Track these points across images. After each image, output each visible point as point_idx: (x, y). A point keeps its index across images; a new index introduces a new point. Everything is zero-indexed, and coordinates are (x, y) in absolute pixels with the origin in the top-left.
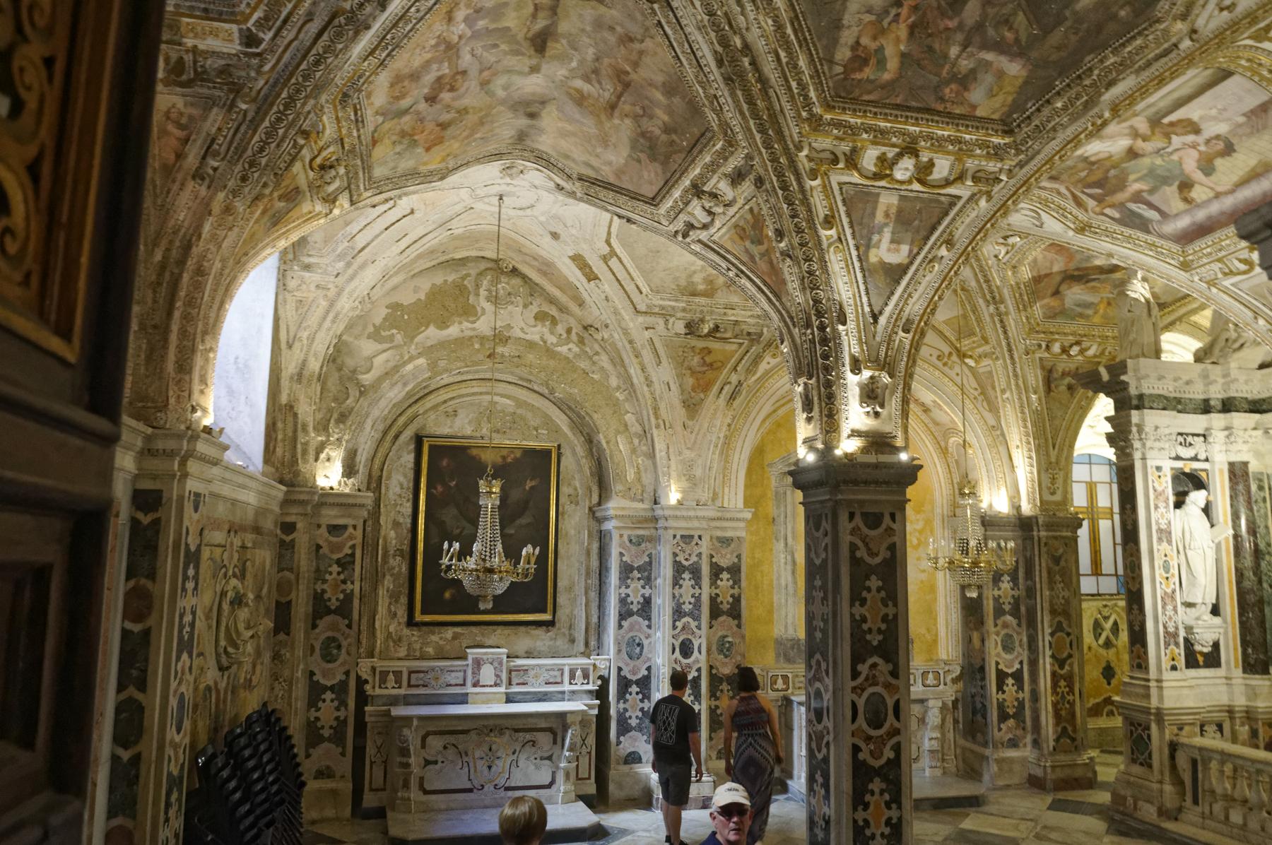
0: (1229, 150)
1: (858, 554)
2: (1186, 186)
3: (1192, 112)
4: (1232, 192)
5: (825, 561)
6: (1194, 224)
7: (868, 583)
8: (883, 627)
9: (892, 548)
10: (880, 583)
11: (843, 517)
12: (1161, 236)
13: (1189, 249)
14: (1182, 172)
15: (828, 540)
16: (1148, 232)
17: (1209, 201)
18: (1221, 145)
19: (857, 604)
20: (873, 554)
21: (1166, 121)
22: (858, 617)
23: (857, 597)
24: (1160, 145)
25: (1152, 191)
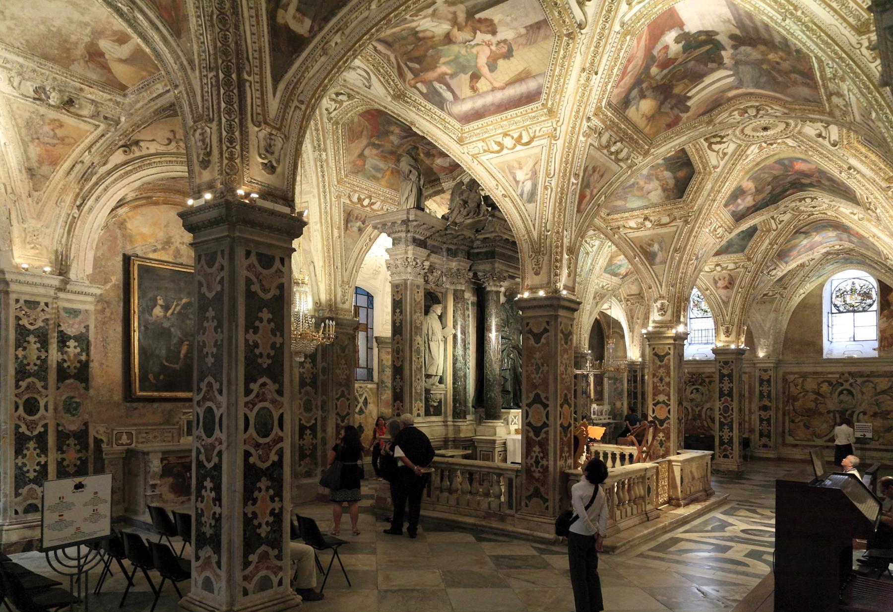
0: (509, 55)
1: (253, 288)
2: (476, 76)
4: (503, 88)
5: (220, 295)
6: (473, 109)
7: (260, 315)
8: (272, 353)
9: (281, 287)
10: (270, 316)
11: (240, 253)
12: (450, 114)
13: (467, 128)
14: (476, 66)
15: (225, 274)
16: (443, 110)
17: (486, 93)
18: (505, 49)
19: (251, 331)
20: (266, 291)
21: (477, 16)
22: (251, 343)
23: (251, 326)
24: (469, 37)
25: (453, 76)
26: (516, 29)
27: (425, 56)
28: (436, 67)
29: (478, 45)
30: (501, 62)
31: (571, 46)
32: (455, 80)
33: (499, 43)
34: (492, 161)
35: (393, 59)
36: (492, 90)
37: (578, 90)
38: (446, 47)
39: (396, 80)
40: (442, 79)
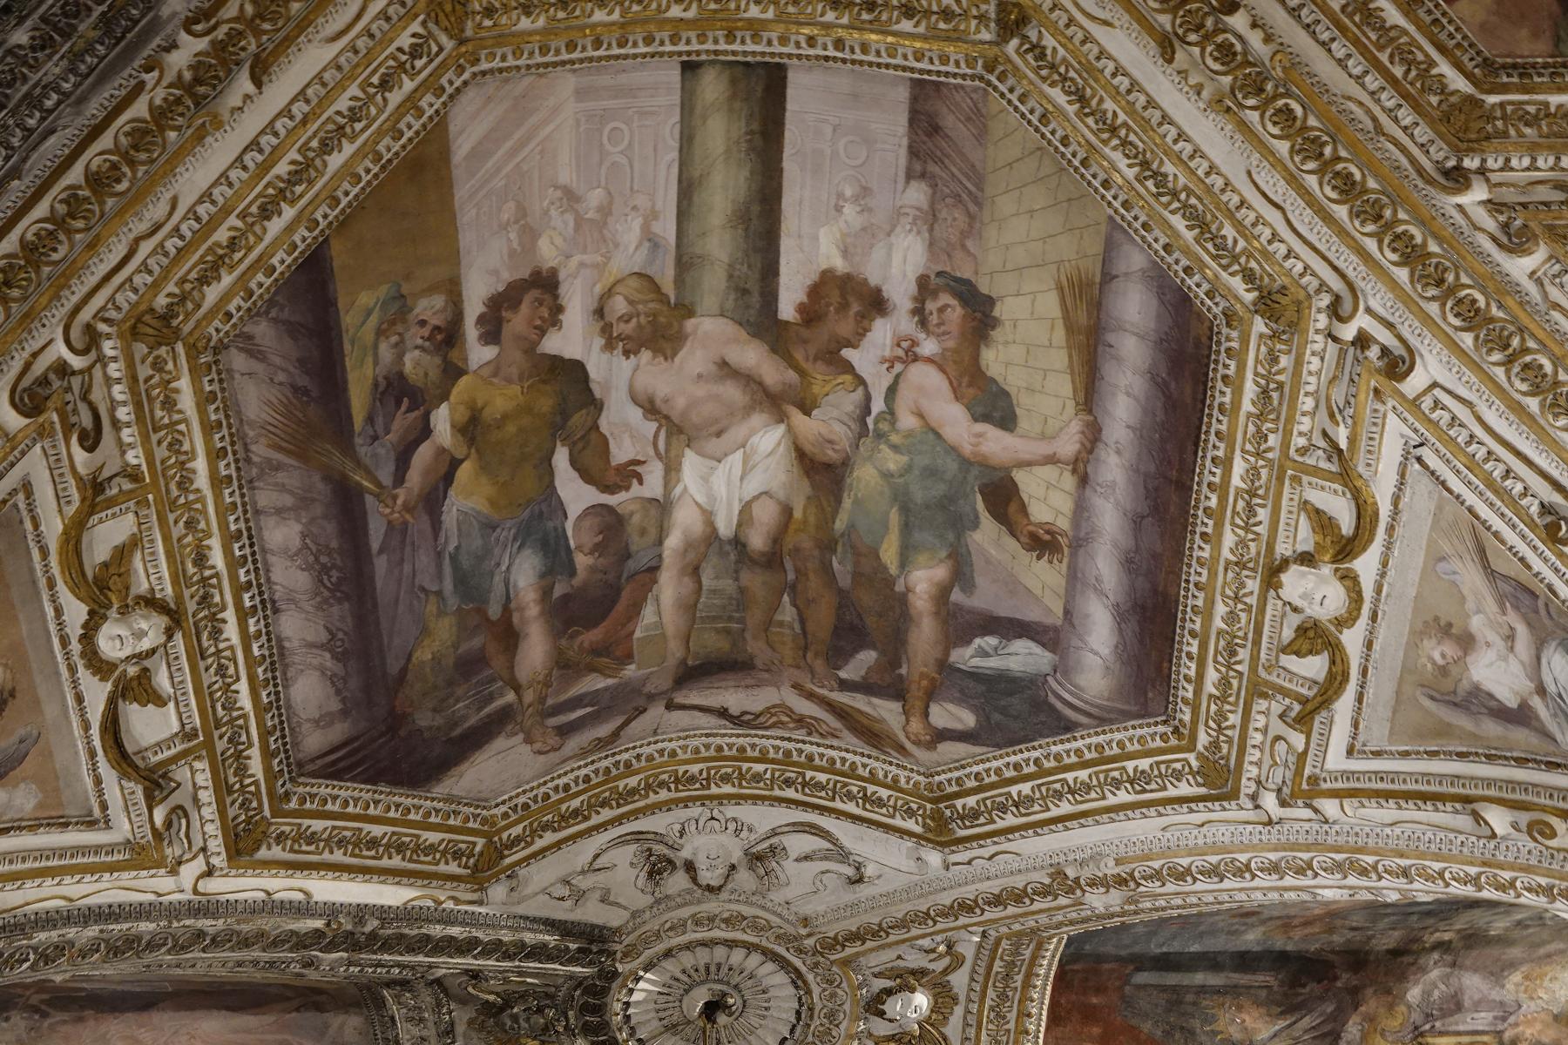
0: (980, 315)
2: (1002, 497)
3: (809, 250)
4: (1093, 435)
6: (1120, 616)
14: (966, 463)
17: (1081, 509)
21: (787, 309)
24: (849, 401)
25: (961, 573)
26: (899, 213)
27: (844, 600)
28: (903, 600)
29: (892, 391)
30: (993, 360)
31: (1049, 42)
32: (980, 580)
33: (919, 312)
36: (1084, 480)
37: (1243, 126)
38: (847, 503)
40: (963, 625)
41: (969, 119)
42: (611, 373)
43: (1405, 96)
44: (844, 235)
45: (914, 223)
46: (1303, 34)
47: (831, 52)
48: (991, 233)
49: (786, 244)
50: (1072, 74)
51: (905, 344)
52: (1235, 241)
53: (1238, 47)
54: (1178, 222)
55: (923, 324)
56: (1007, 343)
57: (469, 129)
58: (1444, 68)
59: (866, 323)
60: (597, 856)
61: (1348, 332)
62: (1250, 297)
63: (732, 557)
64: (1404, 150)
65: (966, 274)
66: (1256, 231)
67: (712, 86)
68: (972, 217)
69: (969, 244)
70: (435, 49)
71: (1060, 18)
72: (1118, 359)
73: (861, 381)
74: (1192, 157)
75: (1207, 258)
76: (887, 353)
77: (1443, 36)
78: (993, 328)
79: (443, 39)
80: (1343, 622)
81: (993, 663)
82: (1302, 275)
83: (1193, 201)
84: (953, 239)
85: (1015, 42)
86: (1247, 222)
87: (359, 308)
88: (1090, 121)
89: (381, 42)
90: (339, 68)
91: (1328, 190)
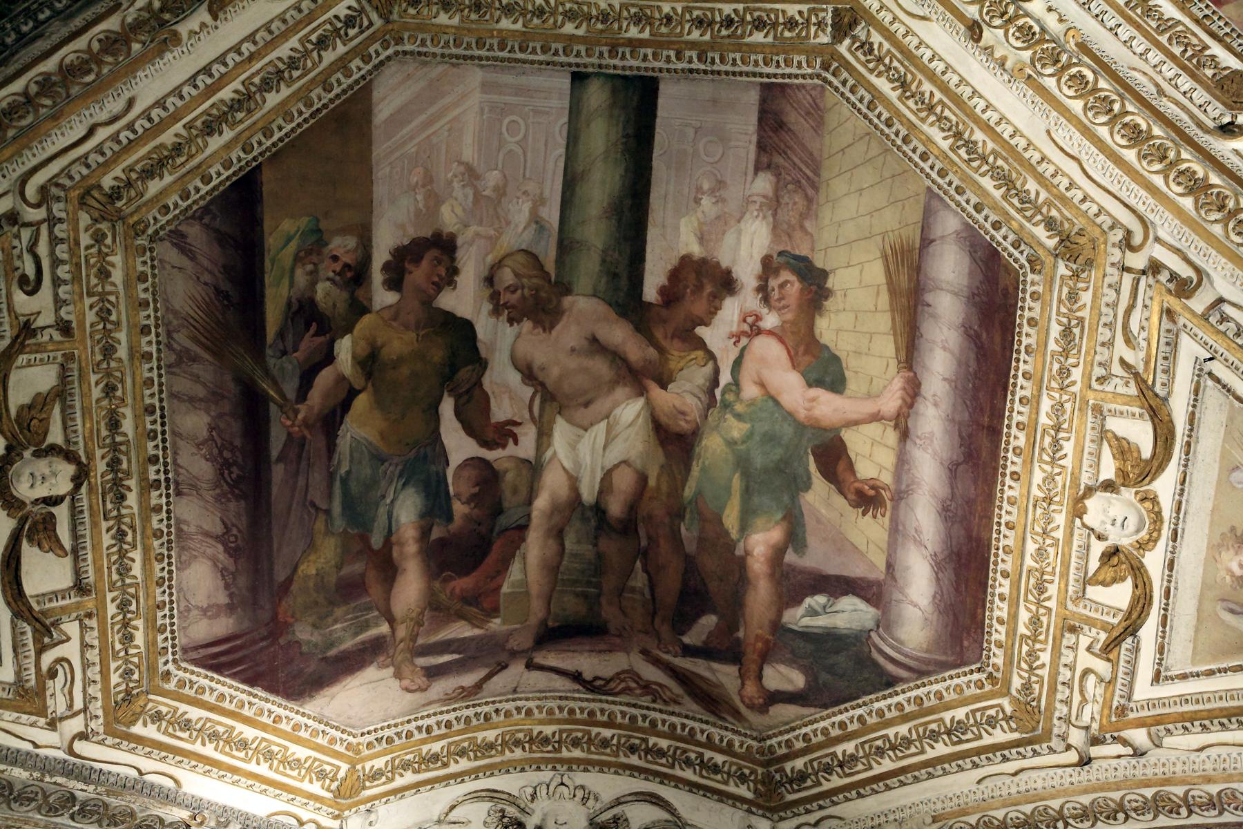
0: (817, 286)
2: (832, 456)
3: (672, 238)
4: (913, 390)
6: (938, 567)
12: (922, 671)
16: (890, 682)
17: (902, 462)
18: (790, 285)
21: (650, 293)
24: (700, 375)
25: (795, 536)
26: (748, 201)
27: (690, 565)
28: (741, 564)
29: (738, 364)
30: (827, 328)
31: (876, 38)
32: (812, 540)
33: (763, 290)
34: (1179, 660)
35: (651, 673)
36: (905, 435)
37: (1042, 91)
38: (696, 470)
39: (716, 733)
40: (797, 585)
41: (808, 113)
42: (498, 337)
43: (1184, 68)
44: (701, 224)
45: (760, 209)
46: (1093, 22)
47: (696, 65)
48: (826, 214)
49: (652, 234)
50: (896, 64)
51: (750, 320)
52: (1038, 194)
53: (1037, 29)
54: (987, 183)
55: (766, 300)
56: (838, 311)
57: (388, 100)
58: (1216, 49)
59: (717, 302)
60: (453, 807)
61: (1137, 261)
62: (1052, 243)
63: (593, 523)
64: (1183, 108)
65: (803, 251)
66: (1055, 181)
67: (596, 95)
68: (809, 200)
69: (807, 224)
70: (366, 23)
71: (885, 17)
72: (934, 316)
73: (711, 356)
74: (998, 124)
75: (1012, 212)
76: (735, 329)
77: (1214, 28)
78: (826, 298)
79: (374, 16)
80: (1142, 546)
81: (822, 621)
82: (1097, 215)
83: (1000, 162)
84: (793, 221)
85: (847, 42)
86: (1047, 174)
87: (282, 232)
88: (911, 103)
89: (322, 7)
90: (284, 21)
91: (1118, 138)
